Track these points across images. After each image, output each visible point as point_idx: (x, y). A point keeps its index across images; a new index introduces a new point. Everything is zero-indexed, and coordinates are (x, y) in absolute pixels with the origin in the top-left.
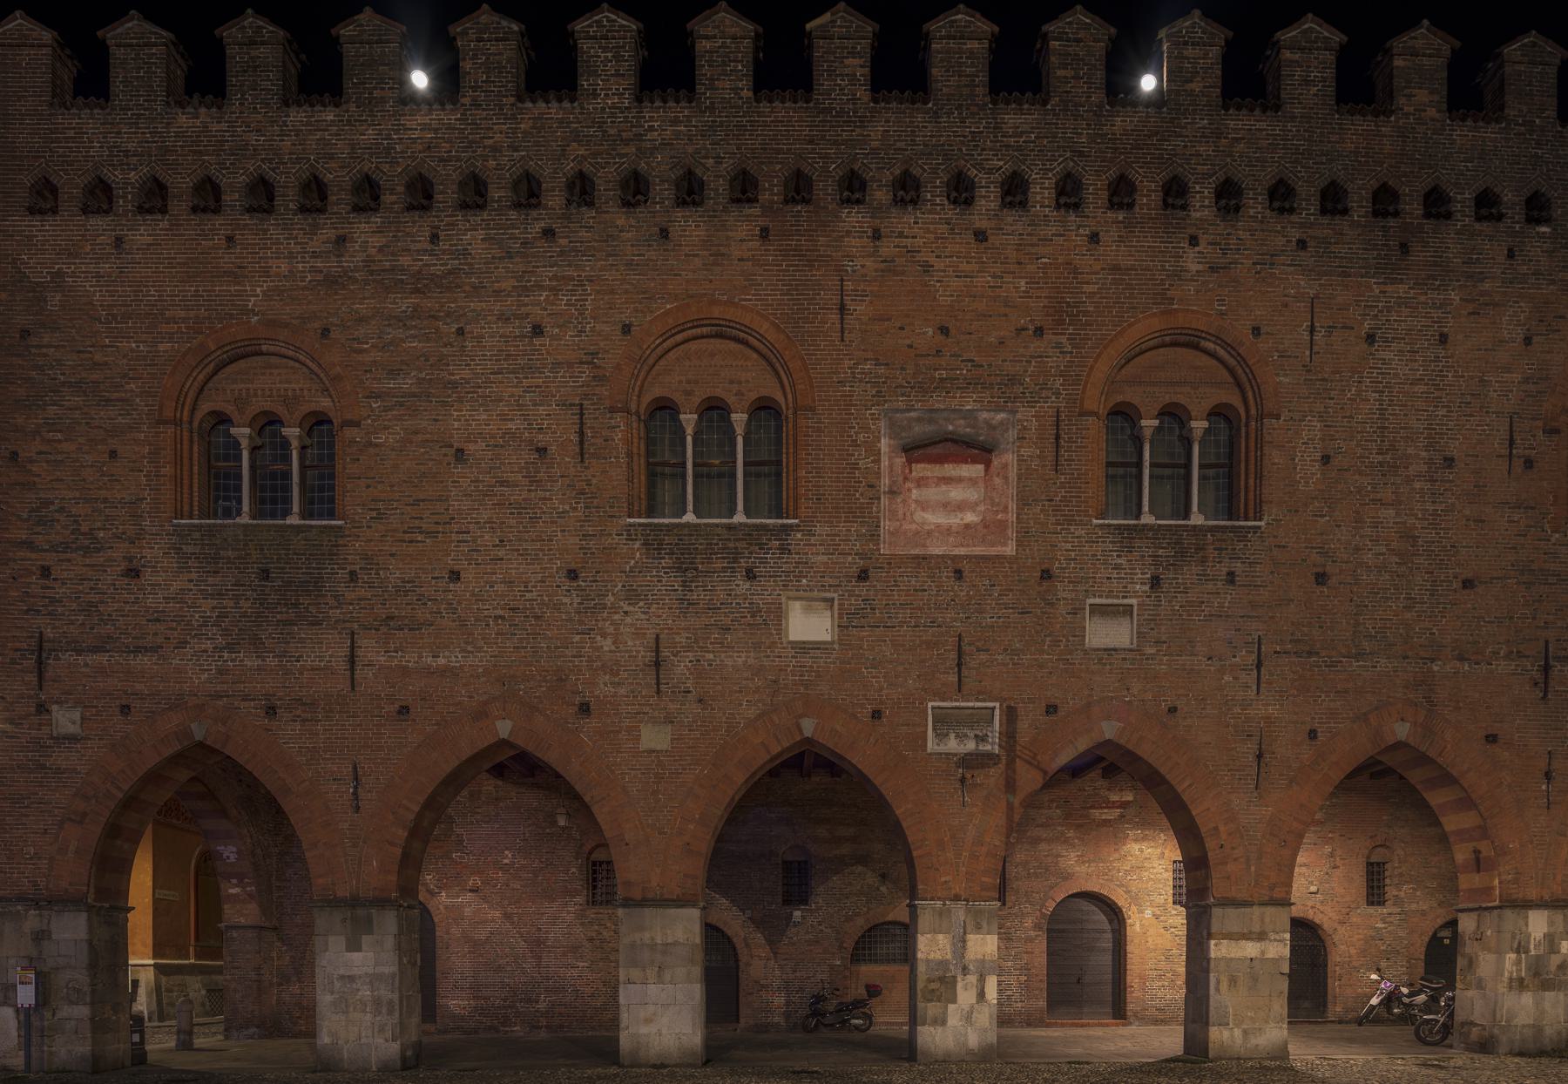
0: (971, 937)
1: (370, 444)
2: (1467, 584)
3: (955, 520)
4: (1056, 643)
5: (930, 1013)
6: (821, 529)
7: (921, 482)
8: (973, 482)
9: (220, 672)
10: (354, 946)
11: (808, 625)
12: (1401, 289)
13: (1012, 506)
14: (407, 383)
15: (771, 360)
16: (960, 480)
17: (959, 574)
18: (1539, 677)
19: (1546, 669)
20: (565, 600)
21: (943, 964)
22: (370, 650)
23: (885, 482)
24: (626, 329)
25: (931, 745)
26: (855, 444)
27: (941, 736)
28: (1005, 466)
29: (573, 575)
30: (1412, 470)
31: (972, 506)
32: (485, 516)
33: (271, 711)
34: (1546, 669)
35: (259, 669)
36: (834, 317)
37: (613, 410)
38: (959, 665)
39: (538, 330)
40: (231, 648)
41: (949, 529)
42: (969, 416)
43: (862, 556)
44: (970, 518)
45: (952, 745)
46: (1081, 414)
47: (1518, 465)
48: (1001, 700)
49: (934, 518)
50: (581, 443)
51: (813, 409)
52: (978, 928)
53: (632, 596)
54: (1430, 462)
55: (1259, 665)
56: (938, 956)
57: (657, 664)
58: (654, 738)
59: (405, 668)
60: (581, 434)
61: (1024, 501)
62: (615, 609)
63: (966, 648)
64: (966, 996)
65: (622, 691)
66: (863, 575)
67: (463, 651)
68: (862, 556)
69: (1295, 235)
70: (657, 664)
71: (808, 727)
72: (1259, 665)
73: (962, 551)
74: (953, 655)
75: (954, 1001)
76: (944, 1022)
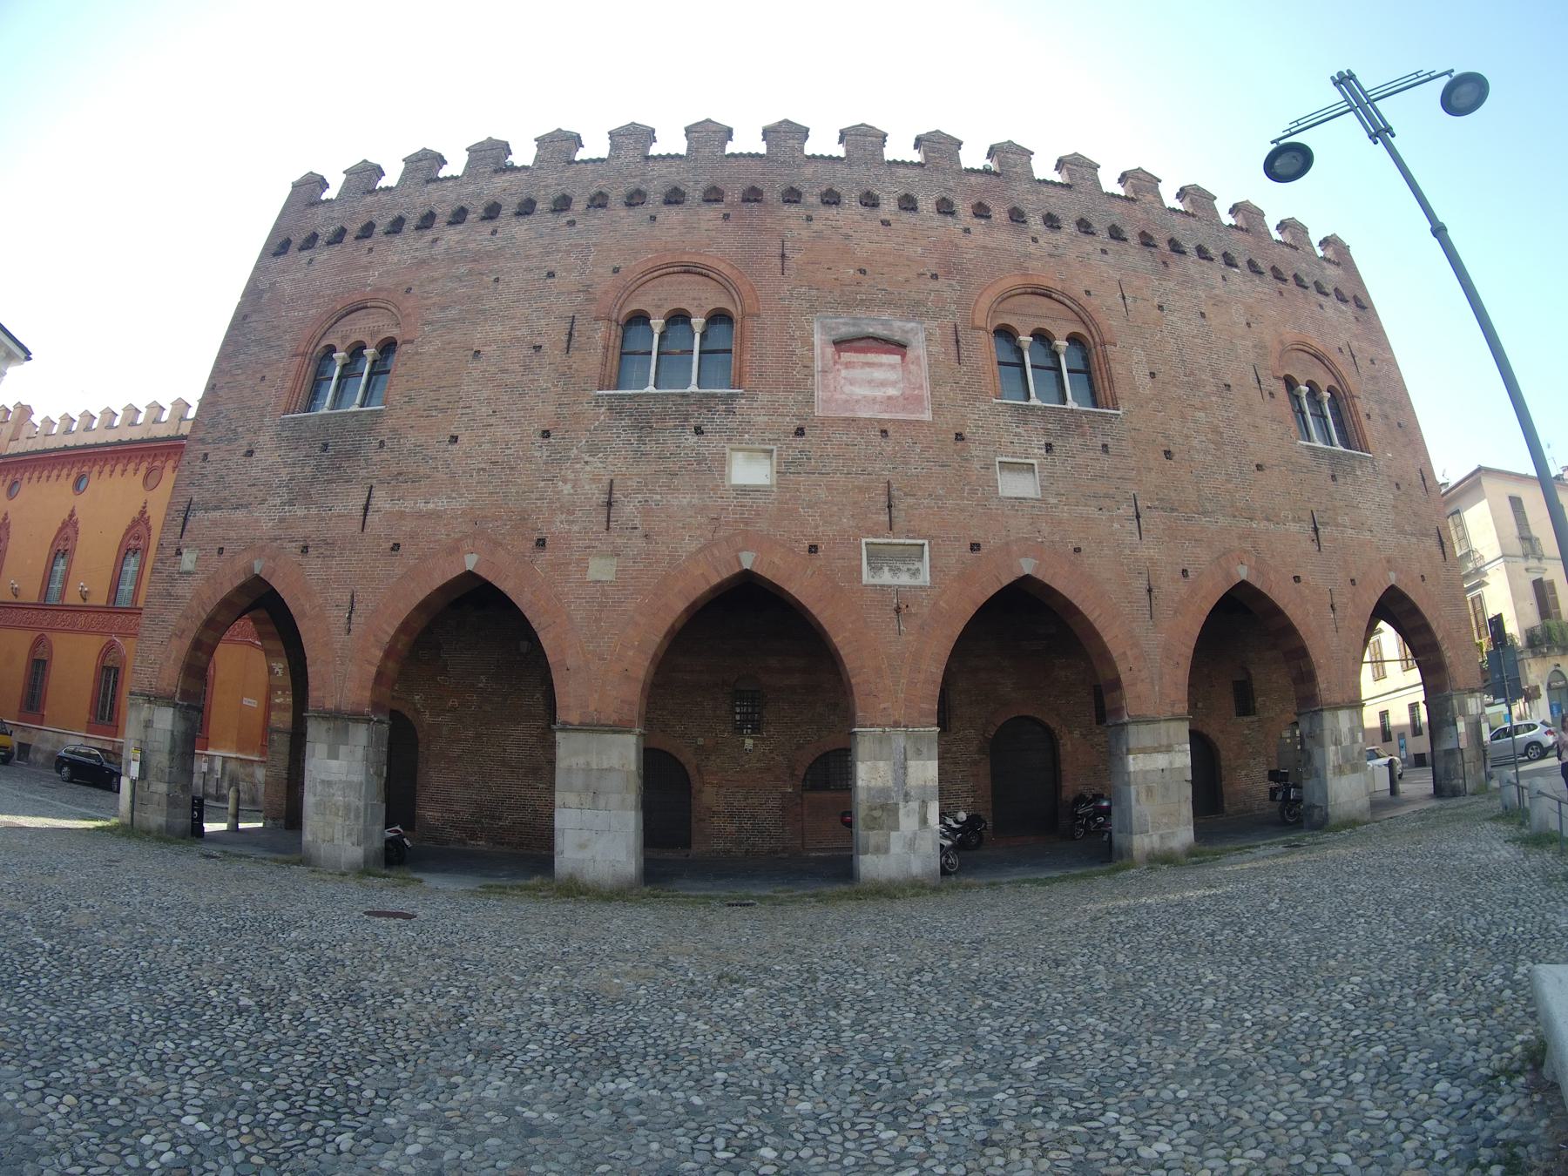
0: (911, 763)
1: (417, 353)
2: (1259, 467)
3: (879, 393)
4: (973, 491)
5: (872, 842)
6: (763, 397)
7: (848, 365)
8: (893, 367)
9: (282, 520)
10: (333, 755)
11: (749, 472)
12: (1171, 285)
13: (926, 384)
14: (453, 313)
15: (725, 284)
16: (881, 365)
17: (884, 433)
18: (1313, 535)
19: (1316, 530)
20: (538, 454)
21: (885, 792)
22: (381, 500)
23: (818, 365)
24: (616, 270)
25: (867, 577)
26: (792, 338)
27: (875, 569)
28: (918, 358)
29: (546, 434)
30: (1208, 389)
31: (894, 384)
32: (485, 394)
33: (305, 550)
34: (1316, 530)
35: (305, 517)
36: (778, 262)
37: (597, 319)
38: (890, 507)
39: (551, 275)
40: (291, 503)
41: (874, 400)
42: (885, 323)
43: (799, 417)
44: (892, 392)
45: (886, 578)
46: (975, 328)
47: (1266, 394)
48: (930, 538)
49: (860, 391)
50: (569, 341)
51: (758, 316)
52: (919, 753)
53: (593, 450)
54: (1217, 386)
55: (1138, 517)
56: (879, 783)
57: (609, 504)
58: (601, 570)
59: (402, 513)
60: (570, 334)
61: (935, 382)
62: (577, 460)
63: (895, 493)
64: (908, 822)
65: (575, 528)
66: (800, 432)
67: (449, 497)
68: (799, 417)
69: (1099, 246)
70: (609, 504)
71: (748, 561)
72: (1138, 517)
73: (886, 416)
74: (884, 499)
75: (897, 828)
76: (887, 851)
